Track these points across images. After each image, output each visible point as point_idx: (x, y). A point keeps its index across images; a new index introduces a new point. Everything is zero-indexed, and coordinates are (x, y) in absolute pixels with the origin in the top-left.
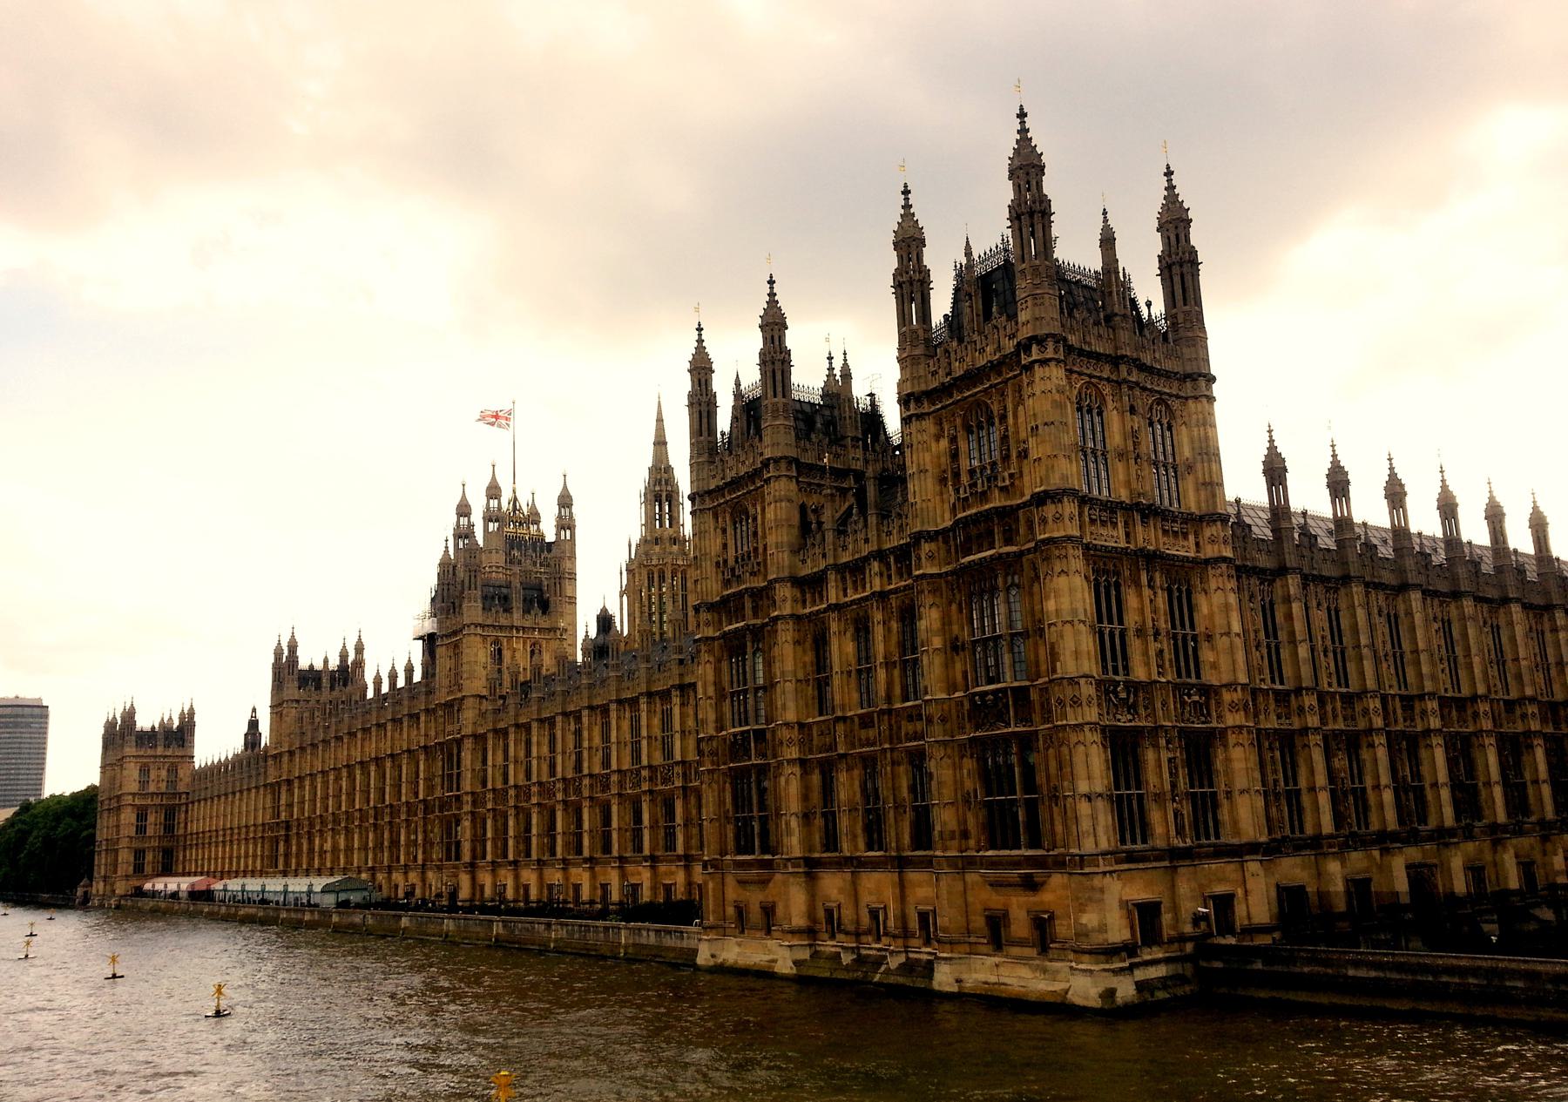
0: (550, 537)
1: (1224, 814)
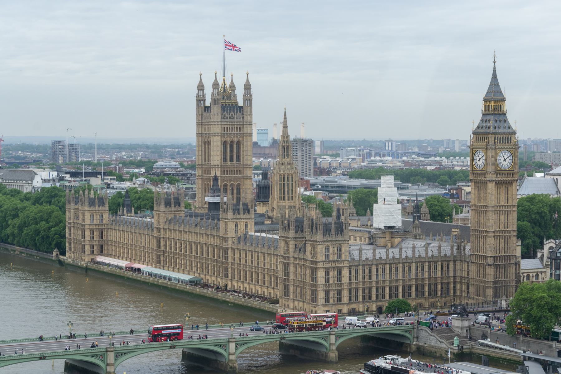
0: (241, 103)
1: (342, 299)
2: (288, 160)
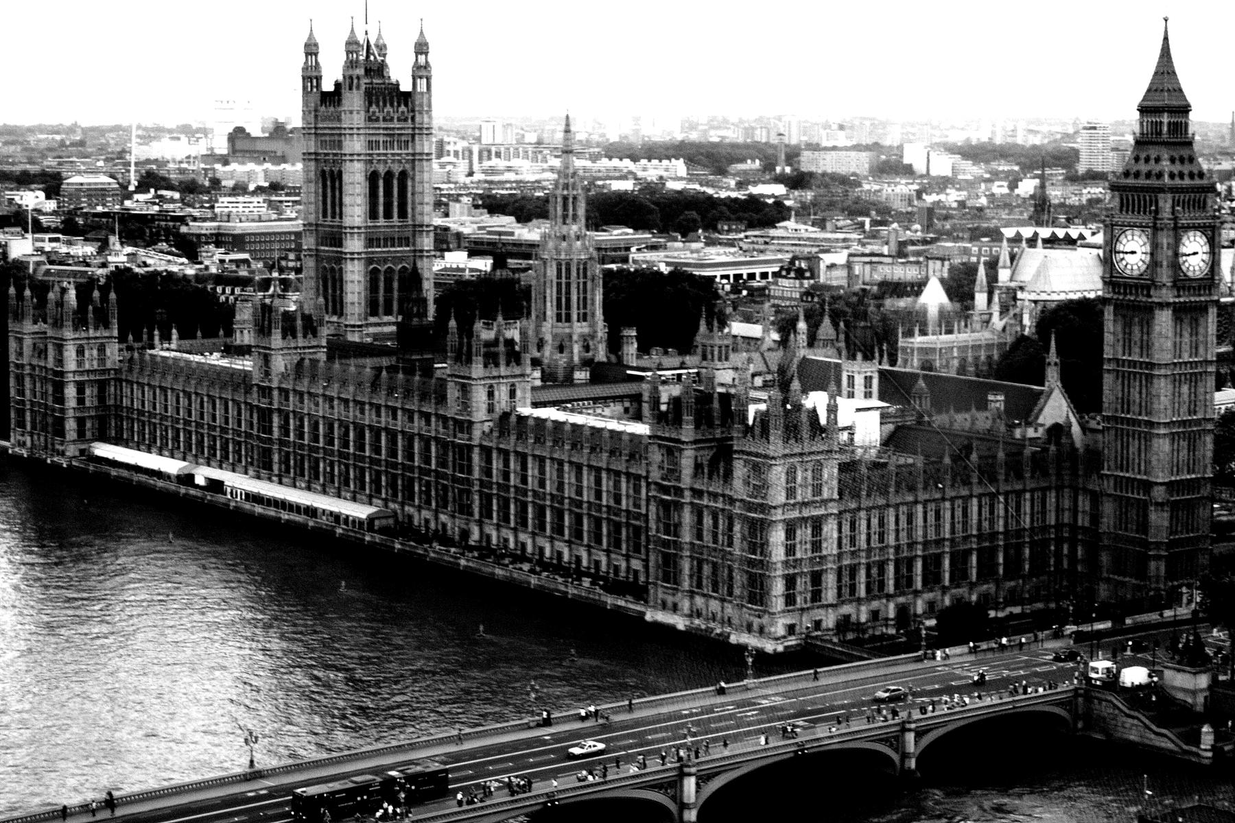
0: (406, 86)
2: (575, 228)
